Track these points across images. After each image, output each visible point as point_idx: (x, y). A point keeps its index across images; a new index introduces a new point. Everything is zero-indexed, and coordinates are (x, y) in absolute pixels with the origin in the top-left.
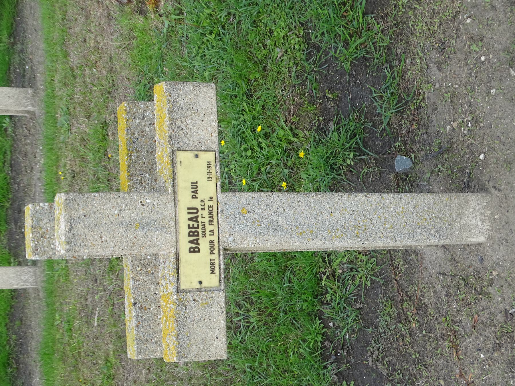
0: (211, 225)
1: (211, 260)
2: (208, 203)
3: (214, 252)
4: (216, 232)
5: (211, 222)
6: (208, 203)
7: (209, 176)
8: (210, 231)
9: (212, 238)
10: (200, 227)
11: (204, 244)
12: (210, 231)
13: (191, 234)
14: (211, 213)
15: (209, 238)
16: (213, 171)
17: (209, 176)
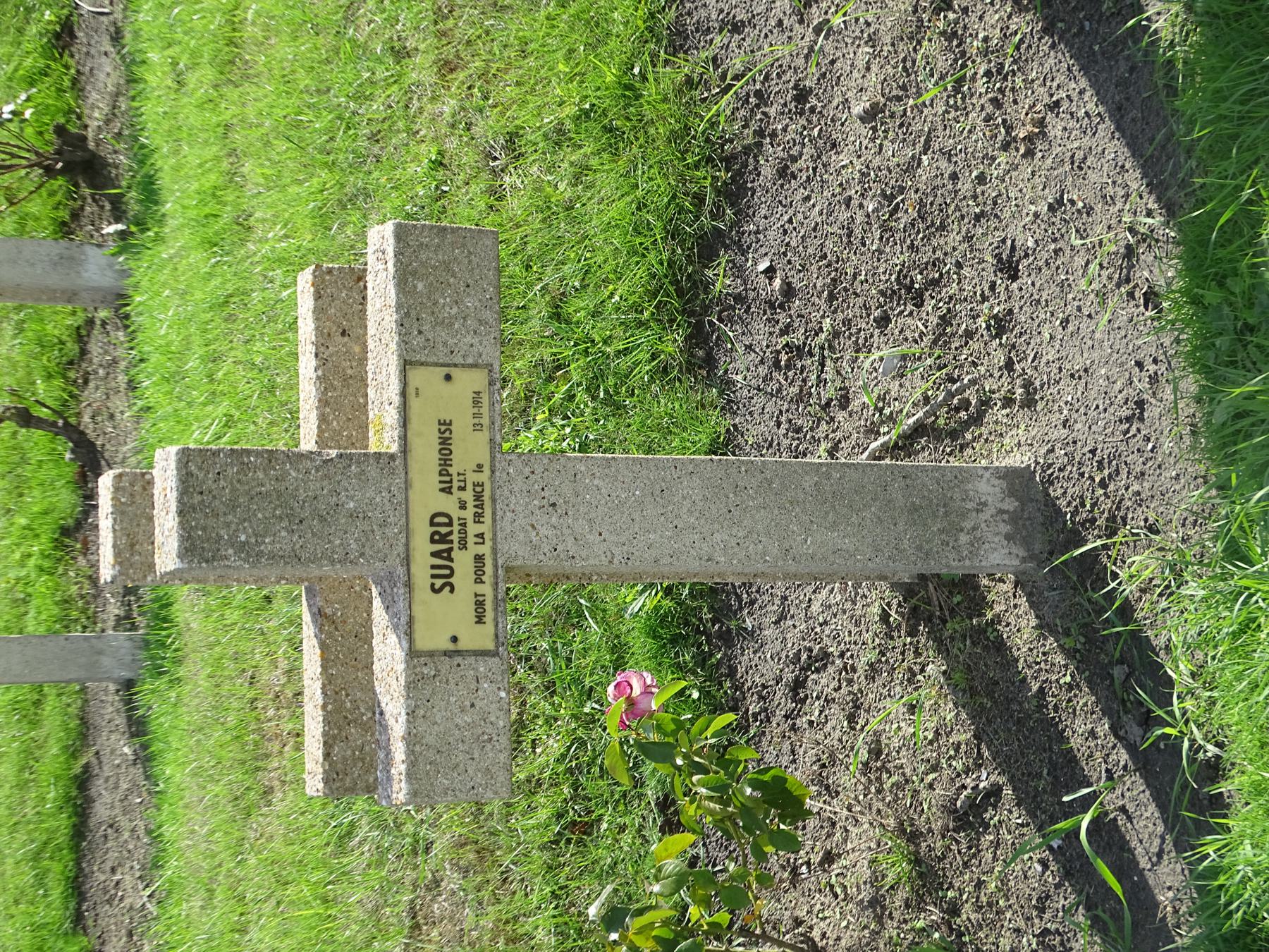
0: (479, 522)
1: (476, 595)
2: (472, 478)
3: (483, 578)
4: (488, 536)
5: (478, 518)
6: (472, 478)
7: (476, 421)
8: (477, 536)
9: (481, 550)
10: (456, 528)
11: (463, 562)
12: (477, 536)
13: (437, 537)
14: (478, 497)
15: (473, 549)
16: (485, 410)
17: (476, 421)
